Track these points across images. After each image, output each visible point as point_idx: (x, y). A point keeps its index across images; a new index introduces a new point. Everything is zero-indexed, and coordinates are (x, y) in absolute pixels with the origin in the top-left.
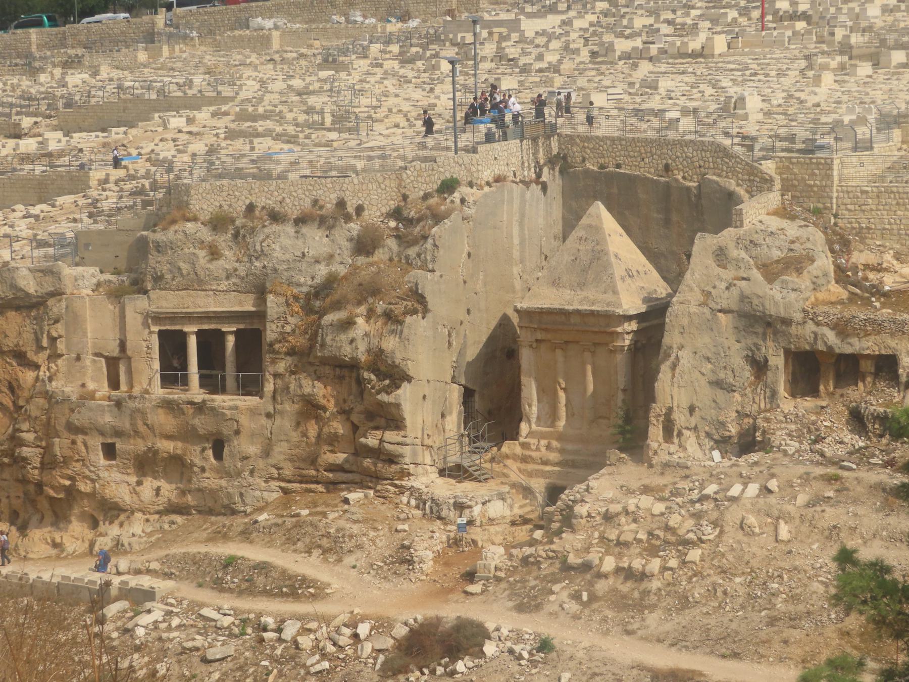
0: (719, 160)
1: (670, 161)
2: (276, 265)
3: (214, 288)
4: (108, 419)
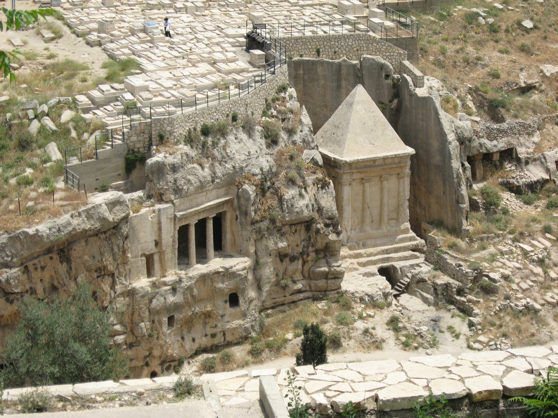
0: (370, 45)
1: (337, 49)
2: (241, 165)
3: (207, 189)
4: (171, 299)
